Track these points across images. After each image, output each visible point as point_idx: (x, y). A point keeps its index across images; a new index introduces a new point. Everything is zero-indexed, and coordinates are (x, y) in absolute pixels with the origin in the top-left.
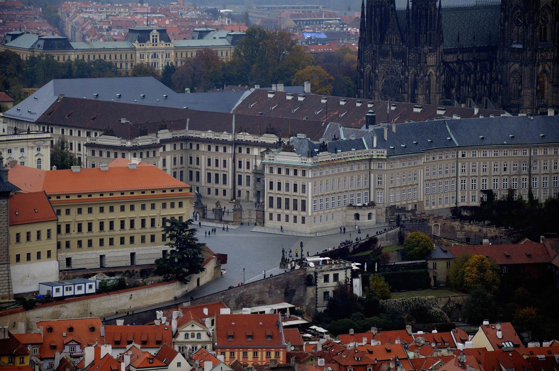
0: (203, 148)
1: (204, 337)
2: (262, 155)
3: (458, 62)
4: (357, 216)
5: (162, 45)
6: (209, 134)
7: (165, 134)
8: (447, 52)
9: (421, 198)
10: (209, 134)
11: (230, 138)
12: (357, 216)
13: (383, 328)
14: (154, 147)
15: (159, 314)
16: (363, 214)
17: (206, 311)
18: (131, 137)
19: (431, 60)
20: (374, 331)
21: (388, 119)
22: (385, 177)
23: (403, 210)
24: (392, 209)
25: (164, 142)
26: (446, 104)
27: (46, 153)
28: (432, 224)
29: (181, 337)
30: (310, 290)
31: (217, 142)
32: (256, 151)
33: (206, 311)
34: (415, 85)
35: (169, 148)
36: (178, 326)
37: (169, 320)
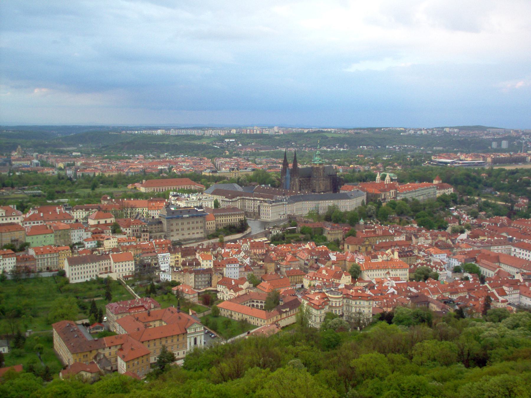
0: (247, 201)
1: (248, 247)
2: (260, 202)
3: (303, 180)
4: (281, 217)
5: (237, 171)
6: (248, 198)
7: (238, 198)
8: (300, 178)
9: (295, 212)
10: (248, 198)
11: (253, 198)
12: (281, 217)
13: (287, 243)
14: (236, 201)
15: (238, 241)
16: (282, 216)
17: (248, 240)
18: (231, 199)
19: (297, 180)
20: (285, 244)
21: (287, 195)
22: (287, 208)
23: (291, 215)
24: (289, 215)
25: (238, 199)
26: (300, 190)
27: (213, 203)
28: (297, 218)
29: (243, 247)
30: (271, 234)
31: (250, 199)
32: (258, 202)
33: (248, 240)
34: (293, 186)
35: (239, 201)
36: (242, 244)
37: (240, 242)
